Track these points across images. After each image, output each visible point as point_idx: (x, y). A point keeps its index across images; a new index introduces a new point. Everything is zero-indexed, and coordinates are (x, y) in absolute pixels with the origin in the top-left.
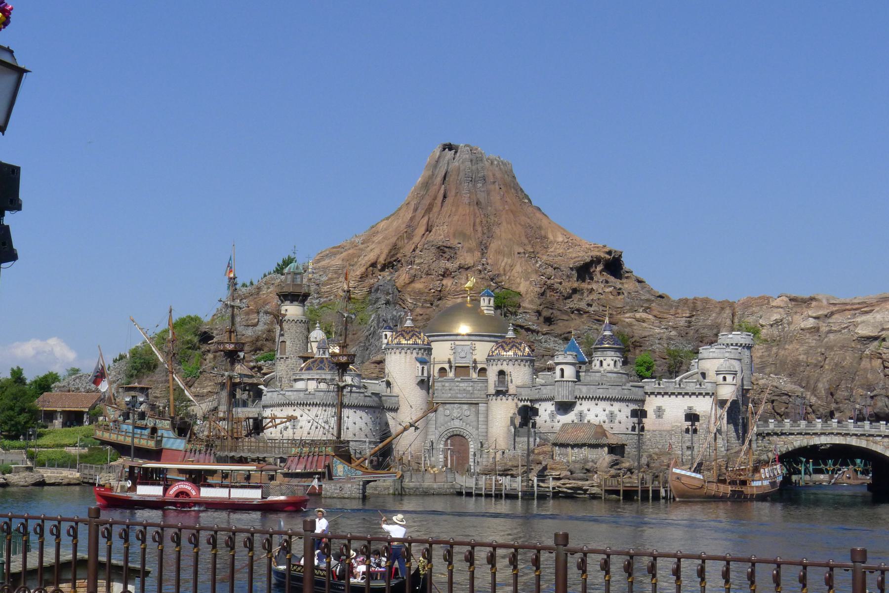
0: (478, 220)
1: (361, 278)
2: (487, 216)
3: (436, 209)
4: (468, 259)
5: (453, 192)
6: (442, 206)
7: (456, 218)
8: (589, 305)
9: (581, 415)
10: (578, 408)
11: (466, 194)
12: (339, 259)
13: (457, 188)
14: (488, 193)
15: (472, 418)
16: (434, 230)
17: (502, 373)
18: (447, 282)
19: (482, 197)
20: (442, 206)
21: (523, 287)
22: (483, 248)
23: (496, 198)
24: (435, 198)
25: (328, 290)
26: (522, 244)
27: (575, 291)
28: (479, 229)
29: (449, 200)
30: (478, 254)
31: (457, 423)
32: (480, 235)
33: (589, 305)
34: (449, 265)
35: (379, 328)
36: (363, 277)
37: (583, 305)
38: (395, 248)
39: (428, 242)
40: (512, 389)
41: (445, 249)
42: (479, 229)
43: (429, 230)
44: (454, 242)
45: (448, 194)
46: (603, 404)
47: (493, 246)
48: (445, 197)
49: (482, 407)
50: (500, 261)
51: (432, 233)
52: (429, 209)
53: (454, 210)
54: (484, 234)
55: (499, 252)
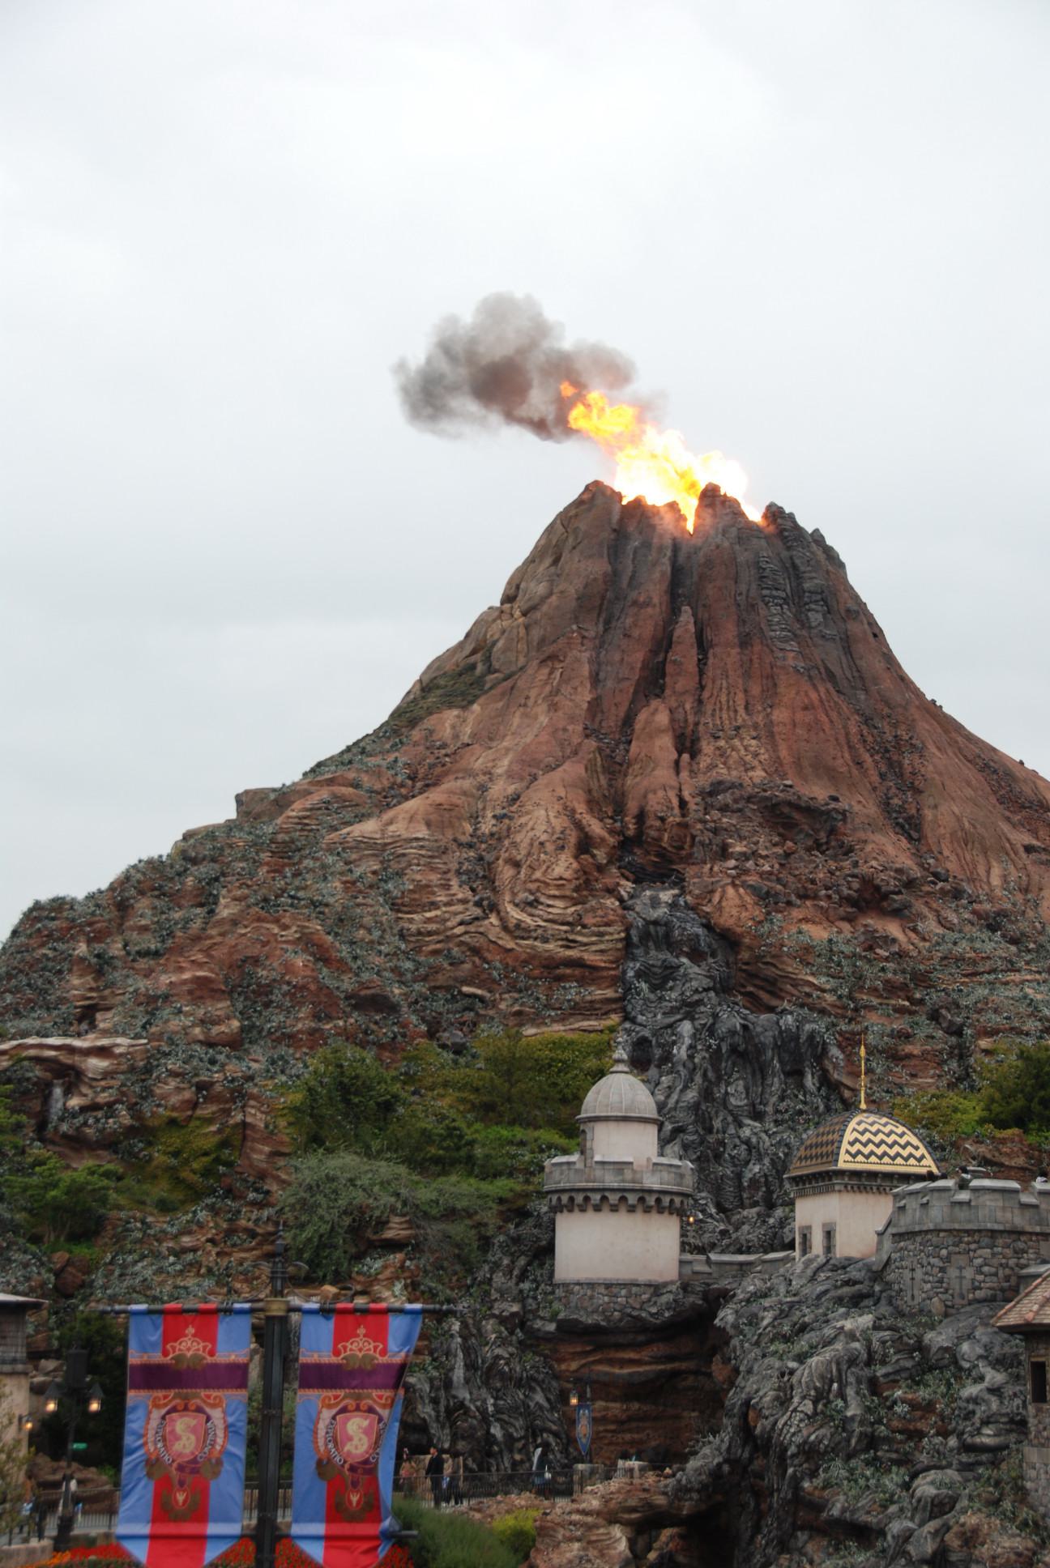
0: (854, 730)
1: (577, 889)
2: (867, 720)
3: (681, 682)
5: (729, 631)
6: (701, 673)
7: (780, 715)
11: (785, 640)
12: (411, 819)
13: (741, 622)
16: (707, 747)
19: (833, 656)
20: (701, 673)
22: (910, 827)
24: (664, 642)
25: (432, 927)
28: (866, 757)
29: (726, 657)
32: (876, 779)
35: (719, 1078)
39: (717, 788)
41: (796, 815)
42: (866, 757)
43: (687, 744)
44: (818, 792)
45: (709, 634)
48: (703, 645)
50: (981, 870)
51: (704, 762)
52: (653, 682)
53: (756, 690)
54: (882, 776)
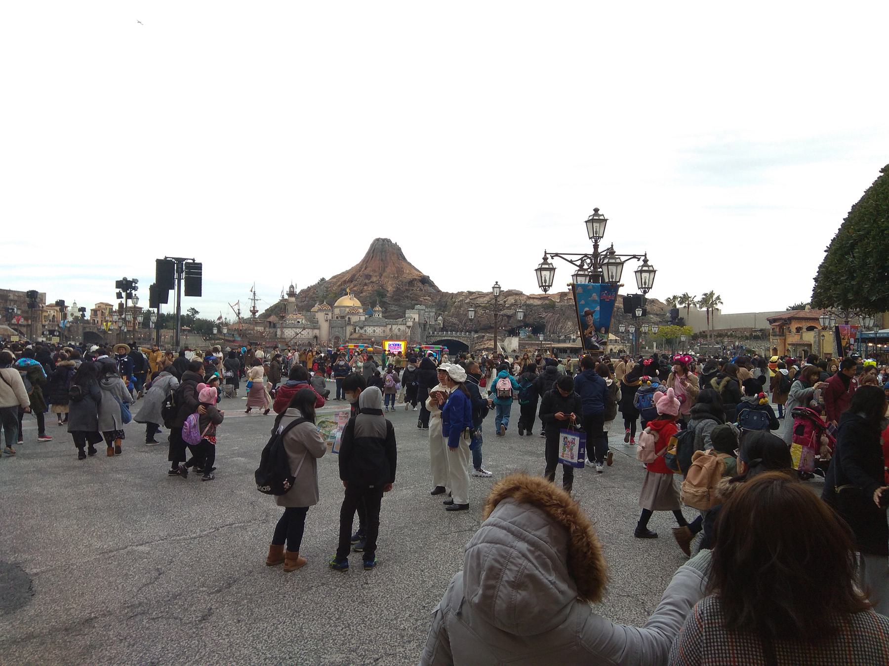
4: (374, 279)
8: (411, 294)
9: (365, 331)
10: (364, 329)
14: (386, 256)
15: (341, 332)
17: (349, 318)
18: (365, 287)
21: (390, 289)
22: (381, 276)
23: (388, 258)
26: (394, 274)
27: (406, 289)
30: (378, 277)
31: (337, 333)
33: (411, 294)
34: (367, 281)
36: (339, 286)
37: (409, 295)
38: (354, 276)
40: (352, 323)
44: (371, 274)
46: (371, 327)
47: (384, 275)
49: (344, 328)
55: (385, 277)
